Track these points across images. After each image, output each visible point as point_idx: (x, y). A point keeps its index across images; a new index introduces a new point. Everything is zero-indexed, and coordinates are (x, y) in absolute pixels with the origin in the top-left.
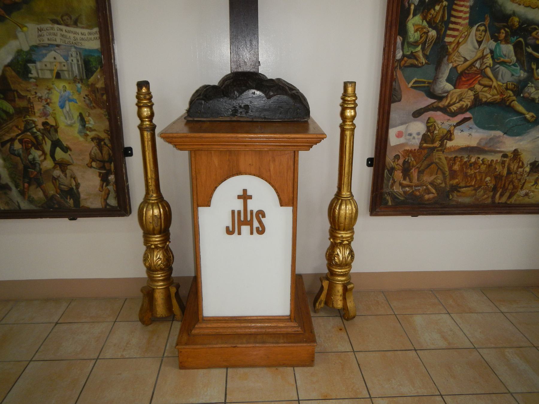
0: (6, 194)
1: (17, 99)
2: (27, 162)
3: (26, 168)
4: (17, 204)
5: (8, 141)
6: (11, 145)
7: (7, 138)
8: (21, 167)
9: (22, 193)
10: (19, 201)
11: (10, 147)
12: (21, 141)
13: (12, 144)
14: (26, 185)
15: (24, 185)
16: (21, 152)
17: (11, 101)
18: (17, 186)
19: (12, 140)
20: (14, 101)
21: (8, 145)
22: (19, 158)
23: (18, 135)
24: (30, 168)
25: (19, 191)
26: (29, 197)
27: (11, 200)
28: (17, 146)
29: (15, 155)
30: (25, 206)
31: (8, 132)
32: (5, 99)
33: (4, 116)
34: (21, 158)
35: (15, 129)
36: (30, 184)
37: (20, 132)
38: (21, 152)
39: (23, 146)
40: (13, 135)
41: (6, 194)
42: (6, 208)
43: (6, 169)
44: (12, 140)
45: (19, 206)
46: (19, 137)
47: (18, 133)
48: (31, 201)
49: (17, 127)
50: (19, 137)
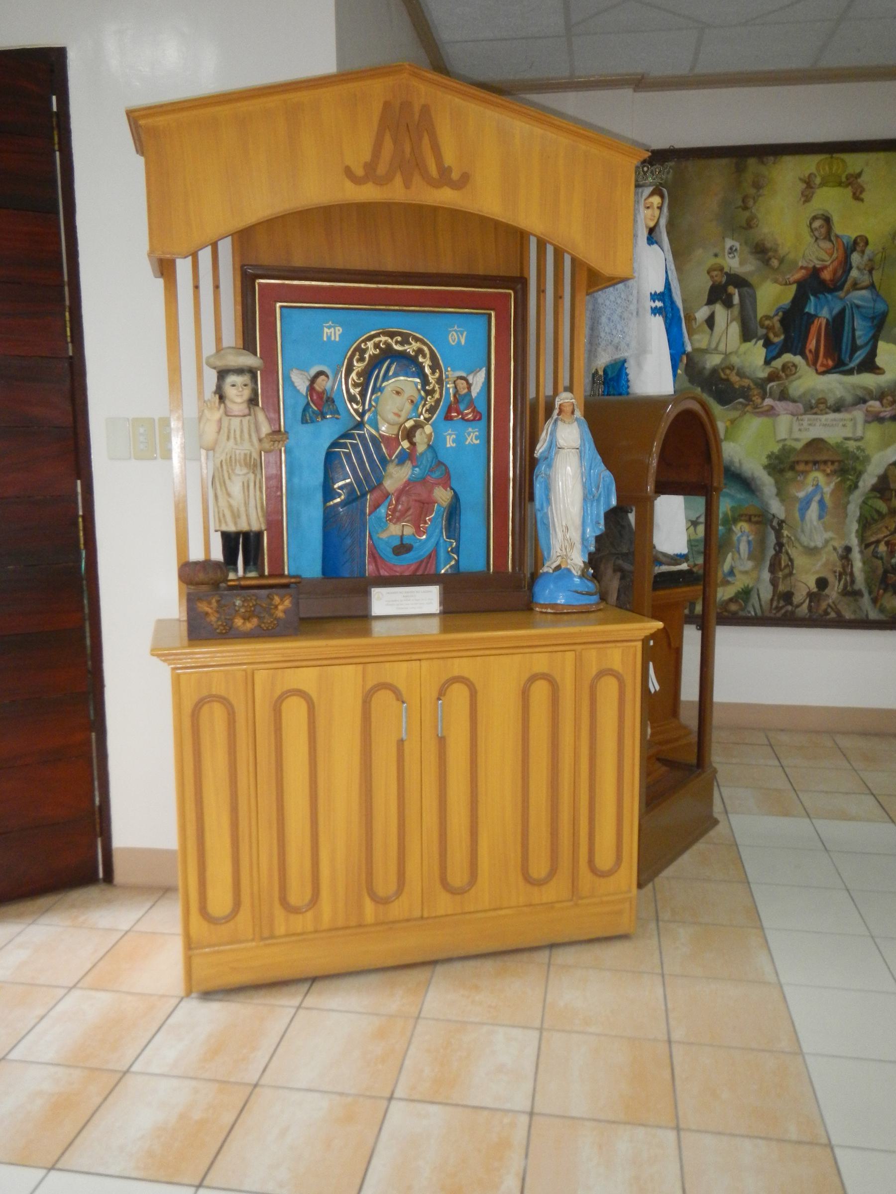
0: (856, 601)
1: (893, 499)
2: (889, 565)
3: (886, 572)
4: (865, 612)
5: (872, 543)
6: (875, 547)
7: (873, 539)
8: (880, 571)
9: (875, 601)
10: (869, 609)
11: (874, 549)
12: (887, 544)
13: (877, 546)
14: (881, 591)
15: (878, 591)
16: (884, 554)
17: (887, 500)
18: (870, 593)
19: (878, 542)
20: (890, 500)
21: (872, 547)
22: (880, 562)
23: (885, 537)
24: (890, 573)
25: (872, 599)
26: (881, 605)
27: (860, 608)
28: (882, 548)
29: (877, 557)
30: (873, 615)
31: (876, 533)
32: (881, 498)
33: (876, 517)
34: (883, 562)
35: (884, 529)
36: (885, 590)
37: (888, 533)
38: (884, 554)
39: (888, 548)
40: (881, 536)
41: (856, 601)
42: (853, 617)
43: (863, 573)
44: (878, 542)
45: (867, 615)
46: (886, 539)
47: (885, 534)
48: (882, 610)
49: (887, 528)
50: (886, 539)
